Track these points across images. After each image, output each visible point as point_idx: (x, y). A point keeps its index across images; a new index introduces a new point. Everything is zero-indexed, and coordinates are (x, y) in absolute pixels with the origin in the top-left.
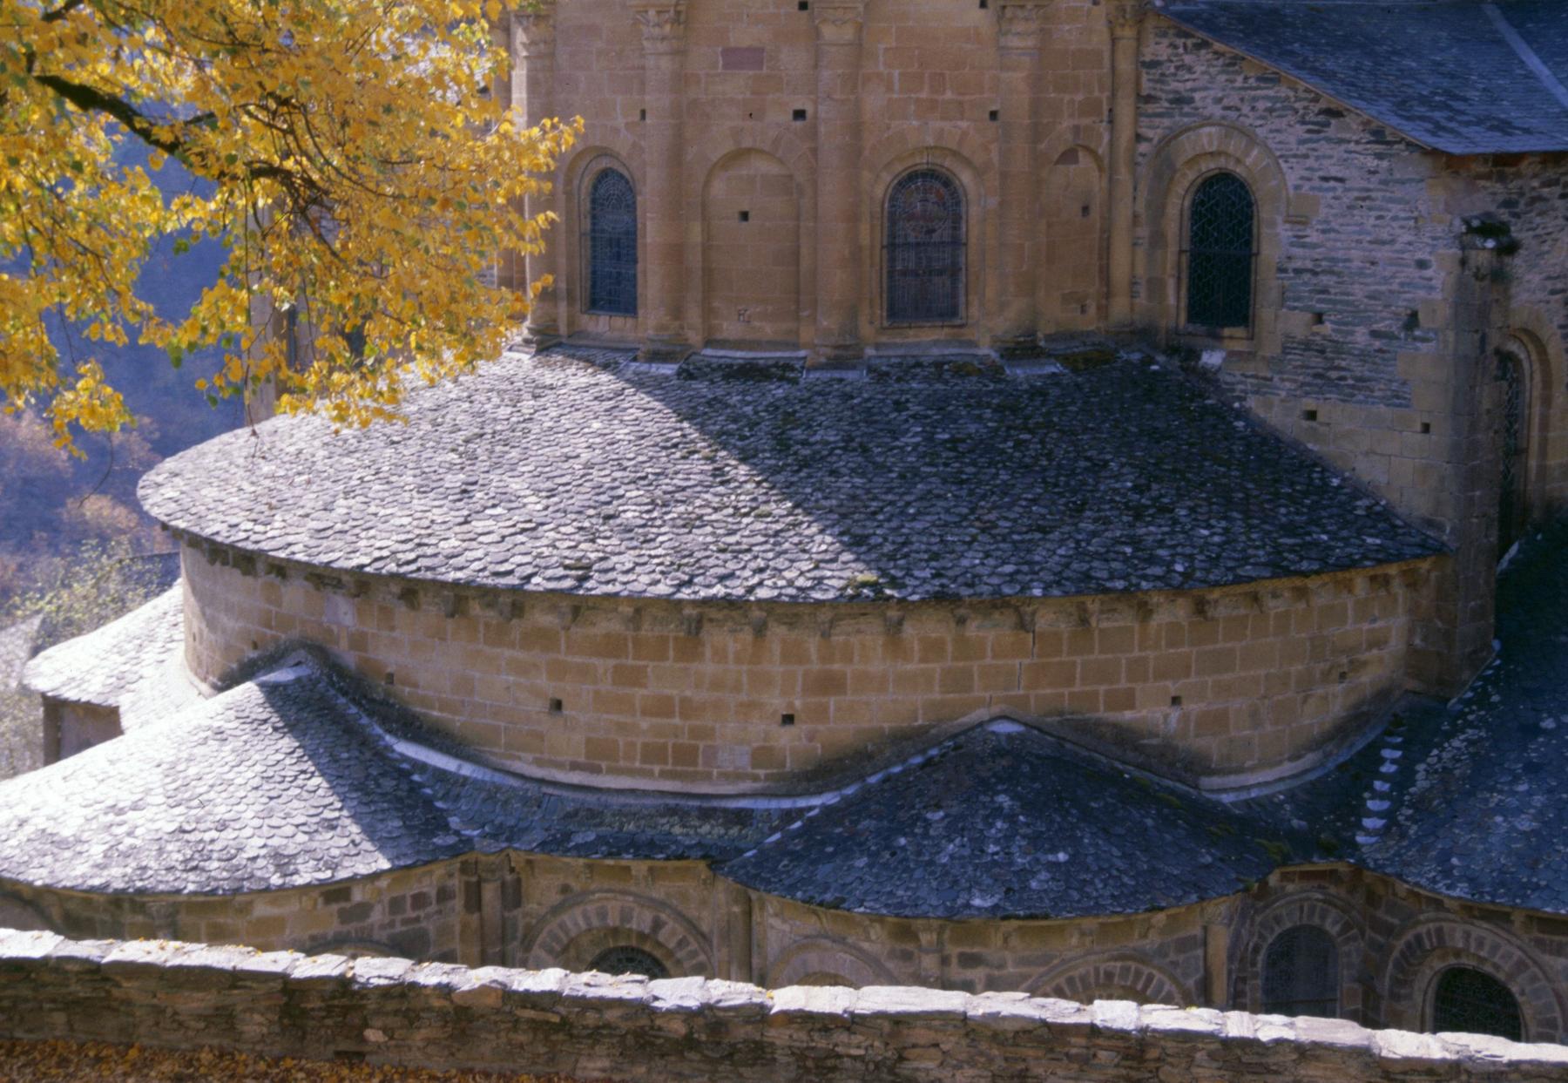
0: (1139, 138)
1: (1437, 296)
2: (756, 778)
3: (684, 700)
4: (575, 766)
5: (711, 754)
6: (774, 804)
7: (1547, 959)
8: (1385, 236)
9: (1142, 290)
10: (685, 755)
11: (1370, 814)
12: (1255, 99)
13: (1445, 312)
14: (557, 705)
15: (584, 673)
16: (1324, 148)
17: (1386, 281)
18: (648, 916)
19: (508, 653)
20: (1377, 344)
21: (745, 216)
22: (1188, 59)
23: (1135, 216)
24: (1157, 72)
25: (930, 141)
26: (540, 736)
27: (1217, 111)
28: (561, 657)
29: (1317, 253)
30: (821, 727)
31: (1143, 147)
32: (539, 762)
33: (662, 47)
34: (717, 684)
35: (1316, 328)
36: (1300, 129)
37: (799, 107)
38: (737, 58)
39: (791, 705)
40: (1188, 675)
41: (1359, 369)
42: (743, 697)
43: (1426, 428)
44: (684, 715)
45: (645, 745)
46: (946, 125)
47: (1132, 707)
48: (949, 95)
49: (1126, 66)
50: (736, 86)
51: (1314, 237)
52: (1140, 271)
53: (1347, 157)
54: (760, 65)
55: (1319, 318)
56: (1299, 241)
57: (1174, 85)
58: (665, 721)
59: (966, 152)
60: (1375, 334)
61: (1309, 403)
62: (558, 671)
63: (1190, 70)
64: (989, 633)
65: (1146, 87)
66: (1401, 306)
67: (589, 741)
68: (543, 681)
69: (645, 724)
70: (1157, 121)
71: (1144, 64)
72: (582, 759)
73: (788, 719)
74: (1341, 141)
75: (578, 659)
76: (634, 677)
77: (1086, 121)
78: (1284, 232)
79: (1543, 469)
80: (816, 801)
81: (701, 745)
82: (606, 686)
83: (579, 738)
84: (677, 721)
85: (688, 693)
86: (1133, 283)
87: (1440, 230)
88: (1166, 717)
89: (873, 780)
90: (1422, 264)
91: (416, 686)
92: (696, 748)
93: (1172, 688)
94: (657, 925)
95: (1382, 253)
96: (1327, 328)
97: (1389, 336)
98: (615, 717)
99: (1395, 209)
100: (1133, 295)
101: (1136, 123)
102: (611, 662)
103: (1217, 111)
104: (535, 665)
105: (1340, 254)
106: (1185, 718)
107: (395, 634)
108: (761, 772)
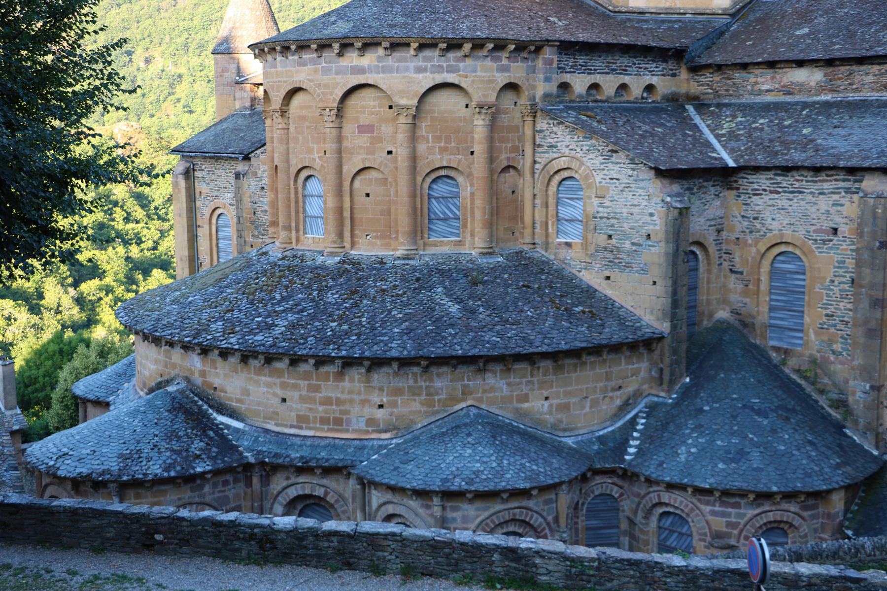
1: (658, 228)
3: (337, 398)
4: (292, 426)
5: (349, 422)
7: (702, 507)
8: (636, 203)
9: (538, 226)
10: (338, 422)
12: (582, 146)
13: (661, 235)
14: (284, 400)
15: (295, 387)
16: (610, 166)
17: (637, 221)
18: (322, 490)
19: (263, 378)
20: (634, 248)
21: (368, 195)
22: (555, 129)
24: (542, 135)
25: (445, 164)
26: (277, 414)
27: (567, 151)
28: (286, 380)
29: (608, 210)
30: (395, 410)
31: (537, 166)
32: (277, 425)
33: (331, 125)
34: (351, 392)
35: (609, 241)
36: (600, 158)
37: (389, 149)
39: (382, 400)
40: (552, 388)
41: (628, 259)
42: (362, 397)
43: (655, 283)
44: (337, 405)
45: (321, 418)
46: (452, 157)
47: (527, 401)
48: (453, 144)
50: (363, 140)
51: (608, 204)
53: (620, 168)
54: (373, 132)
55: (610, 237)
56: (601, 205)
57: (550, 140)
60: (633, 244)
62: (284, 386)
63: (556, 134)
64: (77, 309)
66: (644, 232)
67: (297, 415)
68: (278, 391)
69: (321, 408)
70: (543, 155)
71: (537, 131)
72: (295, 423)
73: (381, 406)
74: (617, 163)
75: (293, 381)
76: (317, 389)
77: (513, 155)
78: (596, 201)
79: (708, 301)
81: (344, 417)
82: (304, 393)
83: (293, 414)
84: (334, 407)
85: (339, 395)
87: (658, 200)
88: (543, 405)
90: (651, 215)
91: (226, 392)
92: (342, 419)
93: (545, 393)
94: (326, 493)
95: (635, 210)
96: (614, 241)
98: (307, 405)
99: (640, 191)
100: (534, 228)
101: (534, 155)
102: (306, 382)
103: (567, 151)
104: (275, 384)
105: (618, 211)
106: (551, 405)
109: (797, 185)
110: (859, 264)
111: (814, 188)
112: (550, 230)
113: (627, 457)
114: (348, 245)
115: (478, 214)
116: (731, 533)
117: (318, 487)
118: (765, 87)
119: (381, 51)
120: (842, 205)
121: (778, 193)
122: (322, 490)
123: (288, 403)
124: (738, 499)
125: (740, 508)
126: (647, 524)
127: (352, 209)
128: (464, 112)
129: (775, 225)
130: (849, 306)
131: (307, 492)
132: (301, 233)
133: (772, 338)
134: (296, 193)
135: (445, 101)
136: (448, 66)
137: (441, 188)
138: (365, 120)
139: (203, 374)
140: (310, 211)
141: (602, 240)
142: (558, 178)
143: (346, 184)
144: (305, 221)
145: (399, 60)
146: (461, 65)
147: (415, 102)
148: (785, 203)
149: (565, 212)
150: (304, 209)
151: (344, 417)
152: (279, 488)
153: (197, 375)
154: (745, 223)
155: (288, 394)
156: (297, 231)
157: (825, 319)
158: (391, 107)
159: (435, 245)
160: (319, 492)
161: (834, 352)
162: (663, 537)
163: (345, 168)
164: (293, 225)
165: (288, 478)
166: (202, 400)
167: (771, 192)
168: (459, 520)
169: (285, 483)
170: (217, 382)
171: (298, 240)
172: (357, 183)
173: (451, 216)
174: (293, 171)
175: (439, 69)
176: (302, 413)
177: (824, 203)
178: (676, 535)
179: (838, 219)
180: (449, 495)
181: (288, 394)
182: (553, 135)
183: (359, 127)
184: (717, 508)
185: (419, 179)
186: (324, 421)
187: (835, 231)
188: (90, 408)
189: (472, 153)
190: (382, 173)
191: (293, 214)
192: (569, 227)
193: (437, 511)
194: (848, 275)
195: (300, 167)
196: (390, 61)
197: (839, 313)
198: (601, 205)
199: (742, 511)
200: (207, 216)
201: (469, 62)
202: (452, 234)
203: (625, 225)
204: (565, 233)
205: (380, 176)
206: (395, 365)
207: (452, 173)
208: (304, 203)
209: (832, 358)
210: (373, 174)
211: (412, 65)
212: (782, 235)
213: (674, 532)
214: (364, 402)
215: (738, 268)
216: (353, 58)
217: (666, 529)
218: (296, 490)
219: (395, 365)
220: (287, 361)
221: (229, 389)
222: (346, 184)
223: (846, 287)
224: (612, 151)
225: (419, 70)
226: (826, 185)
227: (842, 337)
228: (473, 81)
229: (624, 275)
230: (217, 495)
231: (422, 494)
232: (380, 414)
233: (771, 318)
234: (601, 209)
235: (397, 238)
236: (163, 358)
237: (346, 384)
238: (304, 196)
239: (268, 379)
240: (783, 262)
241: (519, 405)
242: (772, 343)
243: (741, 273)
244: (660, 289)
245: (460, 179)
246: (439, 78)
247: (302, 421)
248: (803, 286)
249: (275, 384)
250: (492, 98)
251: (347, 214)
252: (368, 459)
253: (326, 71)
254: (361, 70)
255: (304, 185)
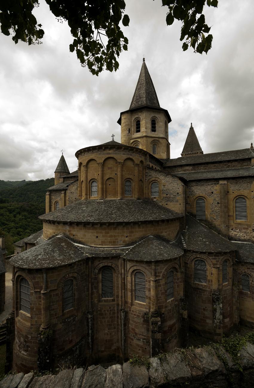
0: (146, 179)
1: (181, 191)
2: (123, 244)
3: (114, 235)
4: (100, 245)
5: (118, 242)
6: (126, 248)
7: (209, 257)
10: (114, 242)
11: (184, 243)
14: (97, 237)
15: (101, 233)
18: (111, 264)
19: (90, 231)
21: (110, 185)
23: (146, 187)
25: (129, 177)
26: (95, 241)
29: (166, 188)
30: (131, 238)
31: (146, 180)
32: (95, 245)
38: (109, 168)
43: (180, 204)
45: (109, 242)
49: (144, 172)
52: (146, 192)
55: (167, 195)
57: (149, 174)
58: (111, 238)
59: (132, 179)
60: (174, 196)
61: (166, 203)
62: (97, 233)
65: (146, 175)
67: (101, 241)
68: (96, 235)
72: (101, 244)
73: (127, 237)
75: (100, 231)
76: (108, 233)
80: (131, 247)
82: (104, 234)
84: (113, 238)
86: (146, 193)
87: (180, 185)
89: (137, 244)
90: (179, 188)
93: (166, 231)
94: (112, 265)
95: (174, 188)
96: (168, 195)
97: (175, 196)
100: (146, 194)
102: (105, 231)
103: (154, 176)
105: (169, 188)
106: (167, 234)
107: (75, 230)
108: (124, 244)
109: (202, 184)
110: (221, 199)
111: (206, 184)
112: (150, 195)
113: (185, 246)
114: (105, 197)
115: (136, 190)
116: (217, 264)
117: (109, 263)
118: (180, 170)
119: (114, 149)
120: (214, 187)
121: (198, 186)
122: (111, 264)
123: (98, 238)
124: (218, 254)
125: (219, 257)
126: (191, 264)
127: (106, 188)
128: (133, 166)
129: (198, 193)
130: (217, 209)
131: (106, 265)
132: (90, 196)
133: (197, 218)
134: (89, 186)
135: (129, 163)
136: (130, 154)
137: (128, 184)
138: (110, 166)
139: (69, 231)
140: (93, 190)
141: (165, 195)
142: (152, 183)
143: (105, 182)
144: (91, 193)
145: (119, 152)
146: (133, 154)
147: (123, 161)
148: (200, 188)
149: (153, 190)
150: (91, 190)
151: (116, 241)
152: (97, 264)
153: (67, 232)
154: (190, 193)
155: (98, 235)
156: (89, 195)
157: (211, 212)
158: (116, 163)
159: (126, 197)
160: (110, 264)
161: (214, 219)
162: (196, 266)
163: (104, 178)
164: (88, 194)
165: (99, 261)
166: (69, 239)
167: (196, 186)
168: (159, 269)
169: (99, 263)
170: (74, 233)
171: (89, 198)
172: (107, 182)
173: (129, 190)
174: (89, 180)
175: (128, 154)
176: (103, 240)
177: (209, 187)
178: (200, 265)
179: (213, 190)
180: (157, 262)
181: (98, 235)
182: (150, 173)
183: (108, 168)
184: (213, 257)
185: (123, 181)
186: (110, 242)
187: (212, 193)
188: (28, 246)
189: (134, 175)
190: (114, 179)
191: (88, 191)
192: (154, 194)
193: (153, 267)
194: (217, 202)
195: (91, 179)
196: (117, 152)
197: (215, 210)
198: (164, 187)
199: (219, 257)
200: (54, 203)
201: (134, 154)
202: (130, 195)
203: (171, 191)
204: (154, 195)
205: (113, 180)
206: (132, 224)
207: (130, 180)
208: (91, 188)
209: (214, 220)
210: (111, 180)
211: (122, 153)
212: (199, 195)
213: (199, 265)
214: (122, 236)
215: (189, 203)
216: (108, 151)
217: (197, 264)
218: (102, 264)
219: (132, 224)
220: (99, 225)
221: (78, 235)
222: (105, 182)
223: (216, 204)
224: (167, 175)
225: (124, 154)
226: (209, 183)
227: (216, 215)
228: (135, 158)
229: (171, 203)
230: (78, 269)
231: (149, 263)
232: (127, 239)
233: (196, 213)
234: (164, 188)
235: (118, 195)
236: (55, 228)
237: (117, 231)
238: (91, 187)
239: (92, 231)
240: (199, 201)
241: (161, 234)
242: (197, 219)
243: (190, 204)
244: (182, 205)
245: (132, 181)
246: (128, 156)
247: (103, 243)
248: (205, 206)
249: (94, 232)
250: (139, 163)
251: (105, 189)
252: (125, 253)
253: (99, 154)
254: (110, 154)
255: (91, 184)
